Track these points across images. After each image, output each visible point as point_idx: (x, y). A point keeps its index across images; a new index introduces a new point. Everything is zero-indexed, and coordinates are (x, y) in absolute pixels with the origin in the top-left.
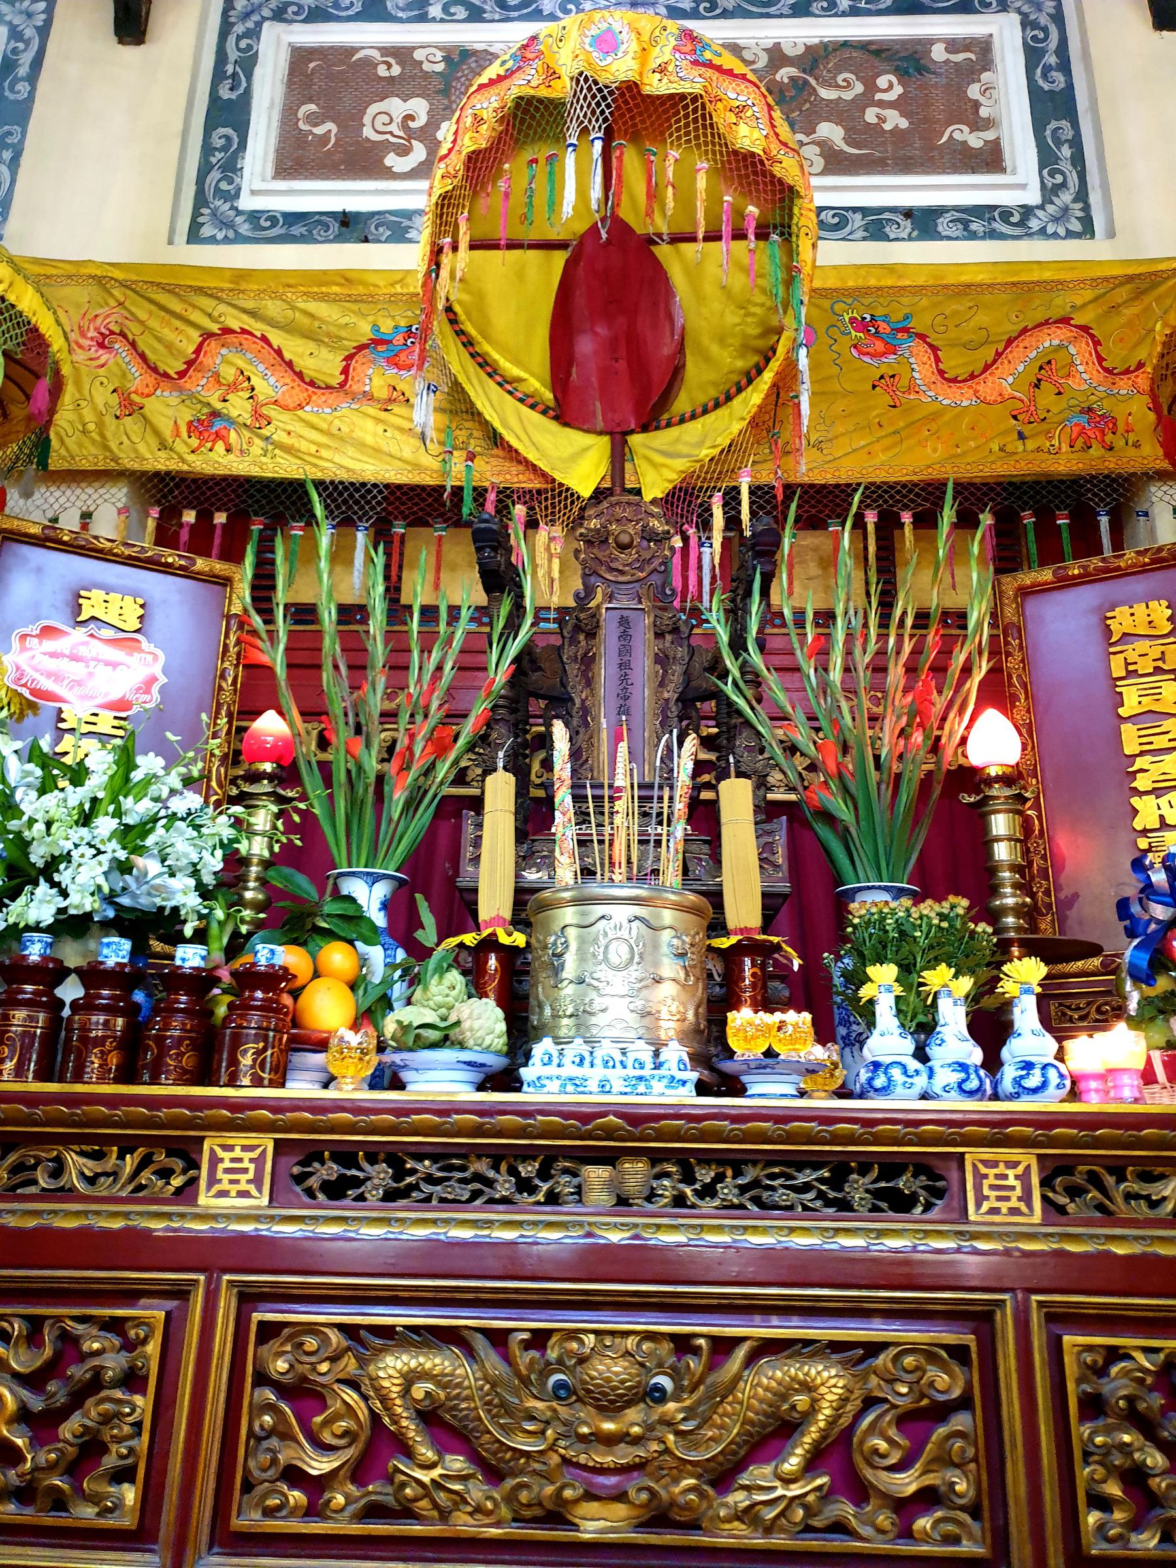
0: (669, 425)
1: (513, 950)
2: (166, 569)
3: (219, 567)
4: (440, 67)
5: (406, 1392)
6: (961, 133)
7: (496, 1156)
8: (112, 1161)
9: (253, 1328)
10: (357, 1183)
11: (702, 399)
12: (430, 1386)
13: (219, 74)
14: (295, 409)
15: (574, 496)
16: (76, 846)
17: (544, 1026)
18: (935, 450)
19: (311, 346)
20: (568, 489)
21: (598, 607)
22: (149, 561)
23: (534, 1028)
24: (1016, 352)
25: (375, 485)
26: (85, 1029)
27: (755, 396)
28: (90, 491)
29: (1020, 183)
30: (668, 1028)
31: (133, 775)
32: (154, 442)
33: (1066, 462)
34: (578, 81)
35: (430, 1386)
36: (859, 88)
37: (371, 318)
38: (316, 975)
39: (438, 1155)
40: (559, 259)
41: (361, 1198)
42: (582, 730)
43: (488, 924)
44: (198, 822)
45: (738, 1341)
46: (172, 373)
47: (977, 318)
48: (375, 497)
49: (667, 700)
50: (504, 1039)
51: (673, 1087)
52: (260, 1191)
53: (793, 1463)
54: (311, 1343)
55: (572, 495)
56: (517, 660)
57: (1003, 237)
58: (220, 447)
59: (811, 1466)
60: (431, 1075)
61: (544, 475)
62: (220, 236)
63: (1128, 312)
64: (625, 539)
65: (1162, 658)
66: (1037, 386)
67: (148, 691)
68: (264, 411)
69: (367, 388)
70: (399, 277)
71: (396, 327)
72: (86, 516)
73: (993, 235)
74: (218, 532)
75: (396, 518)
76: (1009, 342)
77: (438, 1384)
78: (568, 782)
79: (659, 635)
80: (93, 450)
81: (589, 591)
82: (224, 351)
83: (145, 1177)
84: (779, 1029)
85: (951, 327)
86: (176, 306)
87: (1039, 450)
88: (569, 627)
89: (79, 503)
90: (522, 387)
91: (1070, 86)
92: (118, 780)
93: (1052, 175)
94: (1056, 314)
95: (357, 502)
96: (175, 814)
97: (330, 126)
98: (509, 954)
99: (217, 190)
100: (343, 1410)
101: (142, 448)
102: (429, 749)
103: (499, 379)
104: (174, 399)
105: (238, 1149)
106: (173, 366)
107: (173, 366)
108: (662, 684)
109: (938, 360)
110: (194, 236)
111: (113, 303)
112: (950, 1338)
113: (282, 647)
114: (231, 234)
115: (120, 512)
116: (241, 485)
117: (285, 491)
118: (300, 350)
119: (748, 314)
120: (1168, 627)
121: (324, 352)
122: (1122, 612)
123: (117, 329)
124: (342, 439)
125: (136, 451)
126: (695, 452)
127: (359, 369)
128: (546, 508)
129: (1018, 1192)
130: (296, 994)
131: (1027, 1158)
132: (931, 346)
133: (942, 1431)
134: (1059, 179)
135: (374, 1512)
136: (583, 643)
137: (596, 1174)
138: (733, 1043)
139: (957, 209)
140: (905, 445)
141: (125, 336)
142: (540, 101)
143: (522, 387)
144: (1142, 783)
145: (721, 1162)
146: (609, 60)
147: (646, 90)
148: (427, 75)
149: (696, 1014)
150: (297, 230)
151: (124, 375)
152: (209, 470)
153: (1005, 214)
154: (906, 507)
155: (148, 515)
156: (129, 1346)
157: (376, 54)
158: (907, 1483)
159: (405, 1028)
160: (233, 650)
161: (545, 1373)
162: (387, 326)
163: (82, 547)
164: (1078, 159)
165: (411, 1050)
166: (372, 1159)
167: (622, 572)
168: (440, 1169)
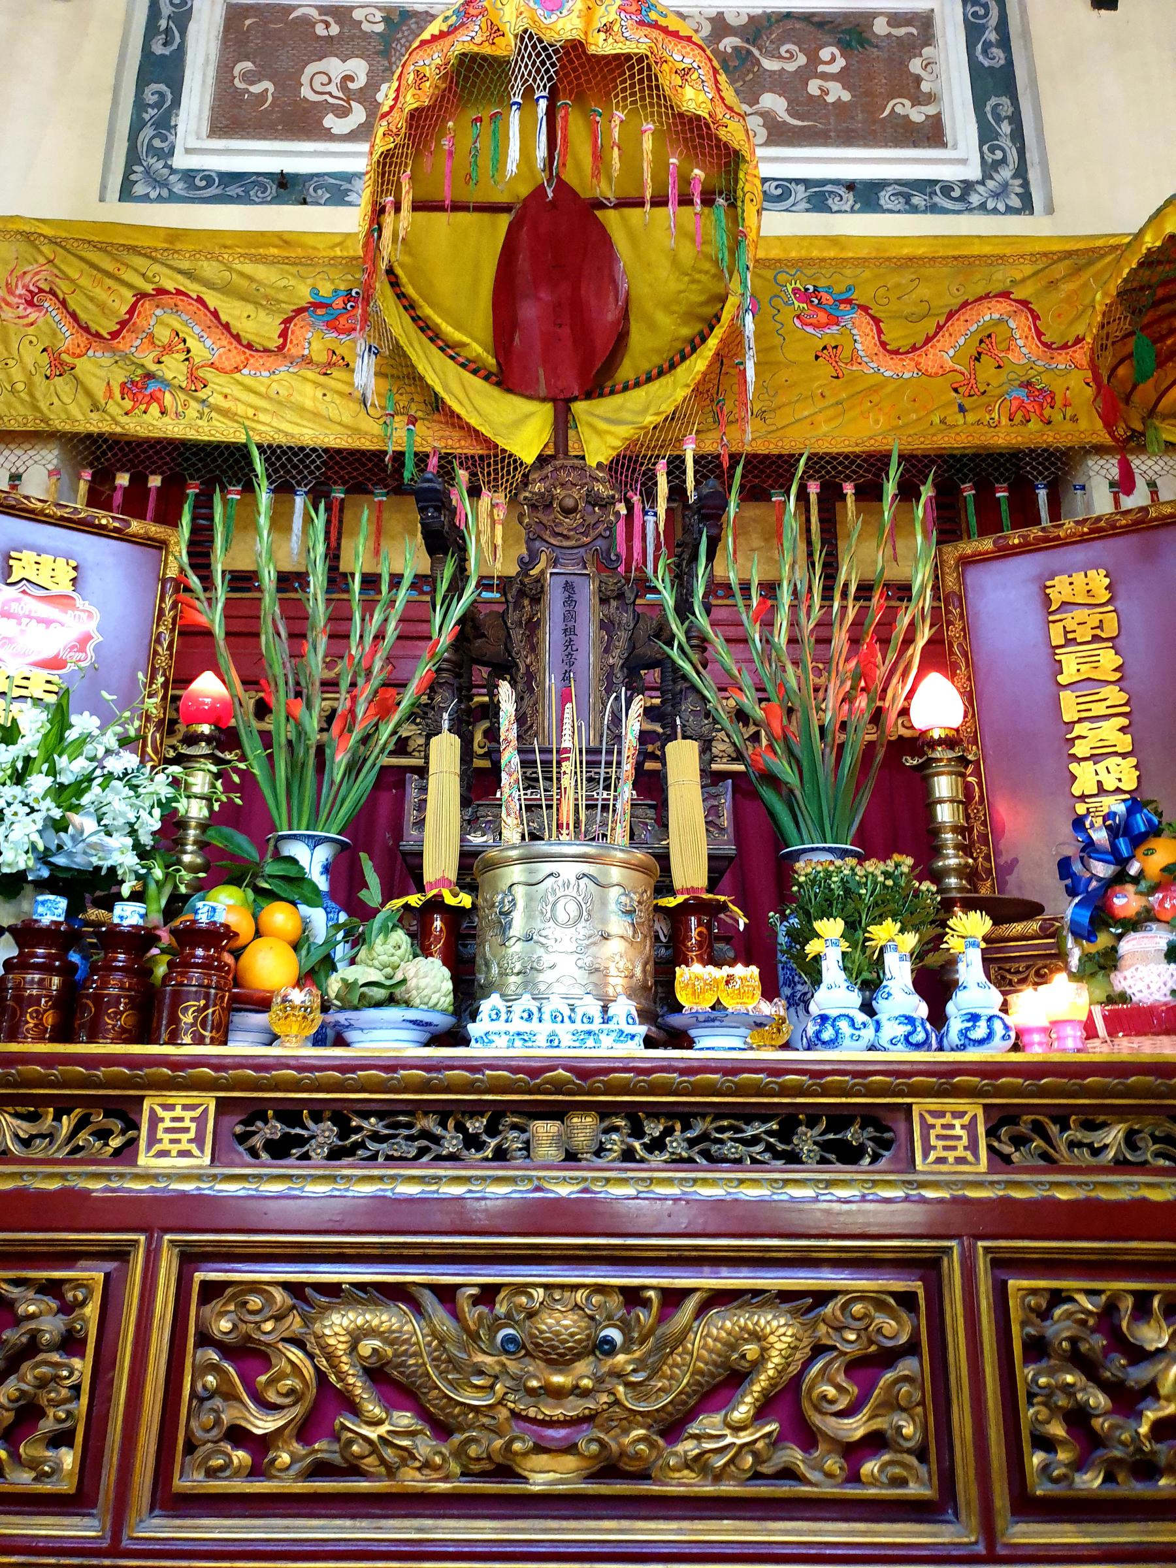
0: (612, 392)
1: (459, 911)
2: (100, 531)
3: (155, 530)
4: (380, 28)
5: (353, 1348)
6: (903, 107)
7: (444, 1112)
9: (196, 1288)
10: (301, 1141)
11: (646, 366)
12: (377, 1343)
13: (151, 29)
14: (232, 372)
15: (517, 463)
16: (9, 804)
17: (492, 984)
18: (877, 422)
19: (249, 309)
20: (511, 456)
21: (543, 572)
22: (82, 522)
23: (481, 987)
24: (957, 325)
25: (314, 450)
26: (18, 988)
27: (699, 363)
28: (18, 452)
29: (959, 159)
30: (617, 983)
31: (67, 733)
32: (86, 403)
33: (1005, 435)
34: (522, 39)
35: (377, 1343)
36: (802, 60)
37: (309, 281)
38: (258, 934)
40: (504, 220)
41: (305, 1156)
42: (526, 696)
43: (432, 886)
44: (135, 782)
45: (687, 1292)
46: (104, 333)
47: (918, 291)
48: (313, 462)
49: (612, 666)
50: (450, 998)
51: (621, 1041)
53: (742, 1411)
54: (255, 1302)
55: (515, 461)
56: (460, 621)
57: (945, 211)
58: (154, 409)
59: (761, 1413)
60: (376, 1034)
61: (487, 440)
62: (153, 195)
63: (1067, 287)
64: (569, 503)
65: (1100, 626)
66: (977, 359)
67: (82, 650)
68: (200, 373)
69: (306, 352)
70: (338, 239)
71: (335, 291)
72: (15, 478)
73: (934, 209)
74: (153, 496)
75: (335, 483)
76: (950, 316)
77: (385, 1341)
78: (515, 743)
79: (604, 601)
80: (22, 411)
81: (534, 557)
82: (159, 312)
83: (82, 1138)
84: (727, 983)
85: (893, 298)
86: (109, 265)
87: (979, 422)
88: (514, 592)
89: (8, 465)
90: (465, 353)
91: (1010, 63)
92: (52, 739)
93: (992, 150)
94: (998, 287)
95: (295, 467)
96: (111, 773)
97: (267, 85)
98: (455, 915)
99: (150, 145)
100: (289, 1369)
101: (74, 410)
102: (372, 711)
103: (441, 343)
104: (106, 360)
105: (179, 1108)
106: (106, 326)
107: (106, 326)
108: (607, 650)
109: (880, 332)
110: (126, 194)
111: (42, 260)
112: (898, 1286)
113: (220, 605)
114: (165, 193)
115: (50, 474)
116: (176, 448)
117: (221, 454)
118: (237, 312)
119: (693, 281)
120: (1105, 596)
121: (262, 314)
122: (1060, 581)
123: (46, 287)
124: (280, 403)
125: (66, 411)
126: (639, 419)
127: (298, 333)
128: (489, 474)
129: (965, 1142)
130: (237, 953)
131: (974, 1109)
132: (873, 318)
133: (889, 1376)
134: (999, 155)
135: (320, 1469)
136: (528, 608)
137: (544, 1129)
138: (682, 997)
139: (898, 182)
140: (848, 416)
141: (55, 294)
142: (484, 58)
143: (465, 353)
144: (1080, 749)
145: (670, 1116)
146: (554, 17)
147: (592, 50)
148: (366, 36)
149: (644, 971)
150: (233, 190)
151: (54, 334)
152: (143, 432)
153: (947, 189)
154: (848, 478)
155: (79, 478)
156: (66, 1308)
157: (314, 13)
158: (855, 1428)
159: (349, 986)
160: (169, 615)
161: (493, 1330)
162: (326, 290)
163: (12, 507)
164: (1018, 136)
165: (356, 1009)
166: (317, 1118)
167: (567, 537)
168: (387, 1127)
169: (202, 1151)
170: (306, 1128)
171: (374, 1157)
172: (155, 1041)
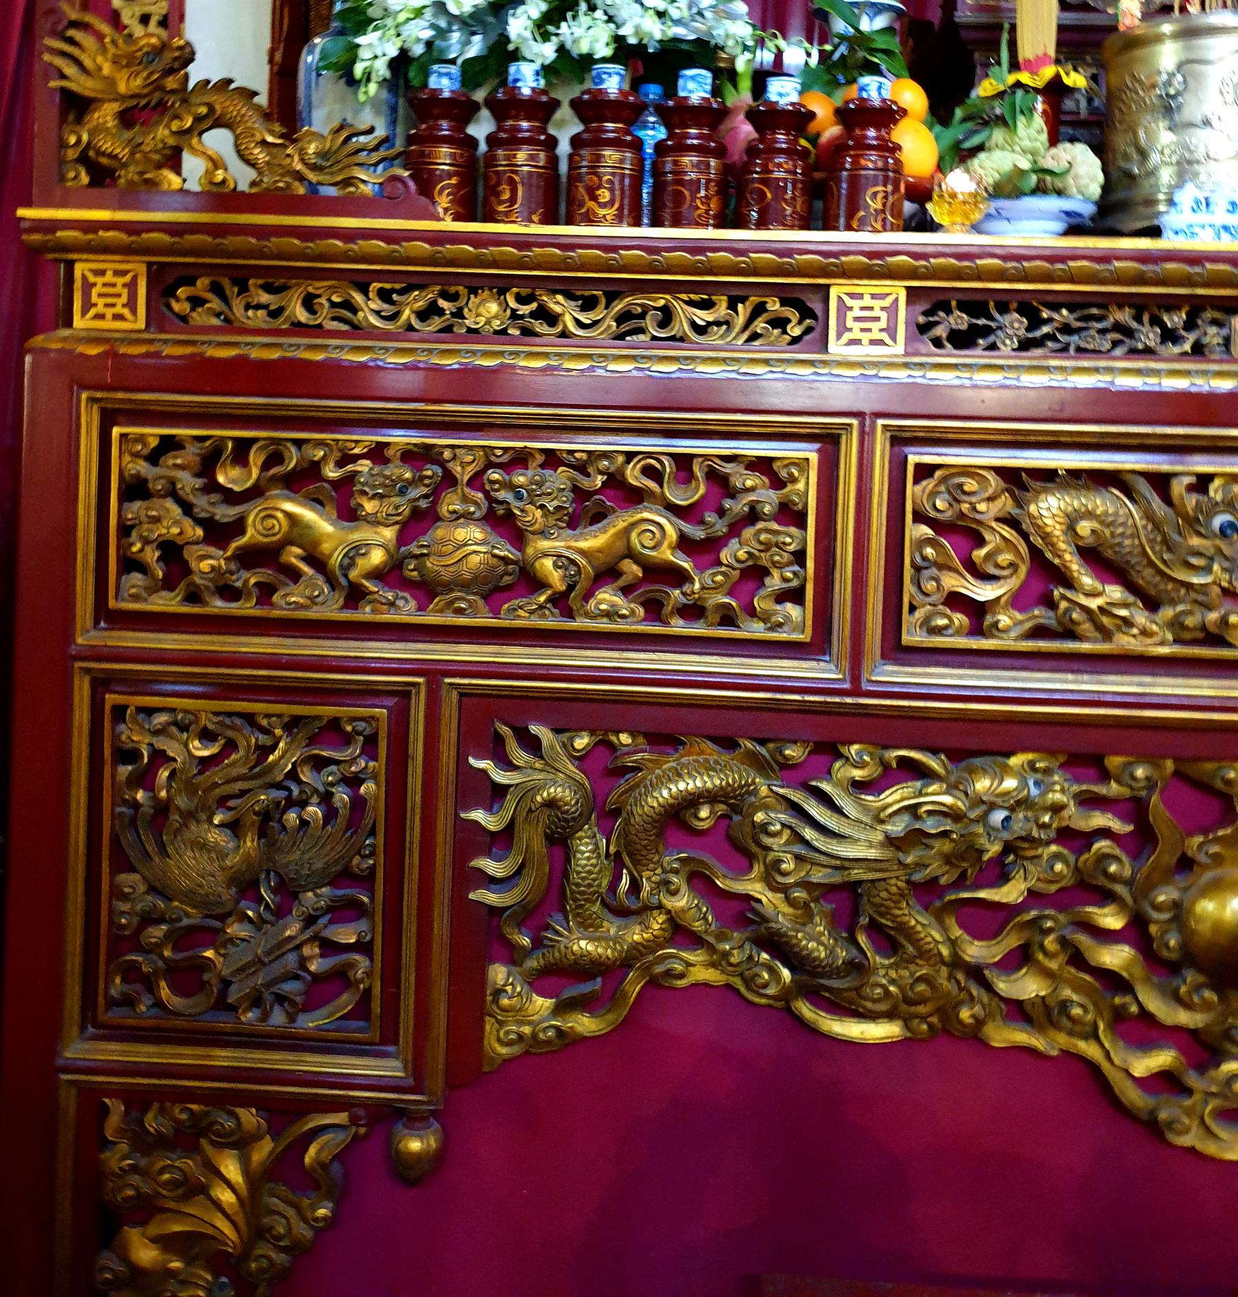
7: (1140, 305)
8: (722, 310)
10: (986, 331)
26: (678, 172)
39: (1075, 303)
41: (993, 347)
52: (894, 339)
83: (760, 325)
156: (778, 483)
166: (1003, 308)
168: (1078, 319)
169: (894, 340)
170: (993, 319)
171: (1065, 349)
172: (836, 228)
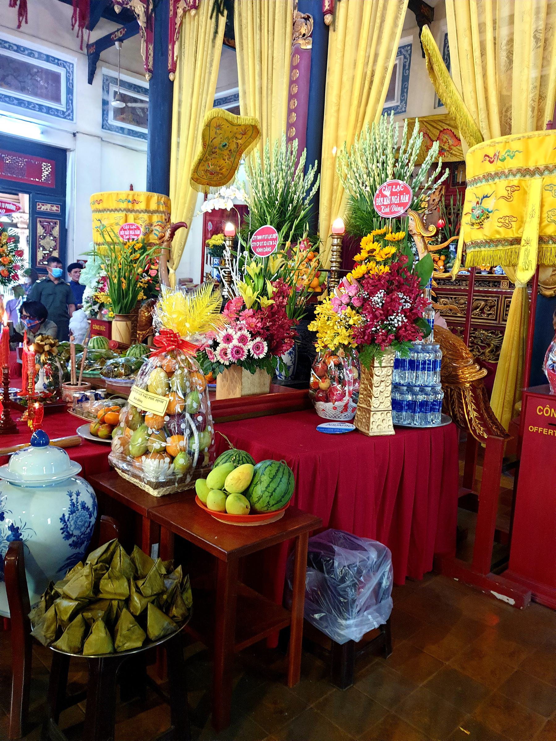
86: (435, 125)
